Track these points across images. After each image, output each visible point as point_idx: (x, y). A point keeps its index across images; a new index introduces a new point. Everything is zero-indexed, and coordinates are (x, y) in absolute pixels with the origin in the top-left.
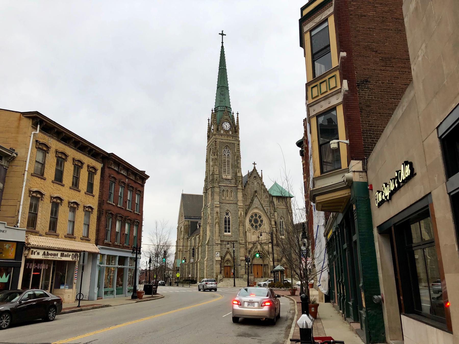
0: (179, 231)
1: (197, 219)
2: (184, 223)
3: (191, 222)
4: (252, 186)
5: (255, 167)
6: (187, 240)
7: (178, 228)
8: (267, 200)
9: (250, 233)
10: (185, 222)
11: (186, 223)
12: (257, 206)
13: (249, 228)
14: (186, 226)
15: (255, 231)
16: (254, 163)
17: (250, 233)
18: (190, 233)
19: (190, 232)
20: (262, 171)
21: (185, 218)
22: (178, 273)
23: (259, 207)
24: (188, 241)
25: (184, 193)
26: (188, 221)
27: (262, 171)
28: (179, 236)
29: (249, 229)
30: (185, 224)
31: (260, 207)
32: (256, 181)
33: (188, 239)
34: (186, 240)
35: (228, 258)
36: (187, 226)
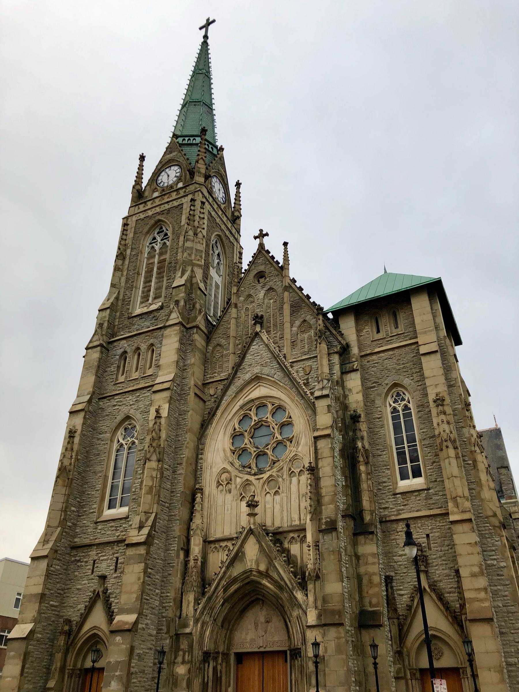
4: (247, 309)
5: (261, 246)
8: (310, 338)
9: (230, 491)
12: (257, 370)
13: (228, 472)
15: (252, 478)
16: (264, 232)
17: (230, 491)
20: (285, 244)
23: (266, 370)
27: (285, 244)
29: (225, 476)
31: (273, 372)
32: (263, 287)
35: (95, 628)
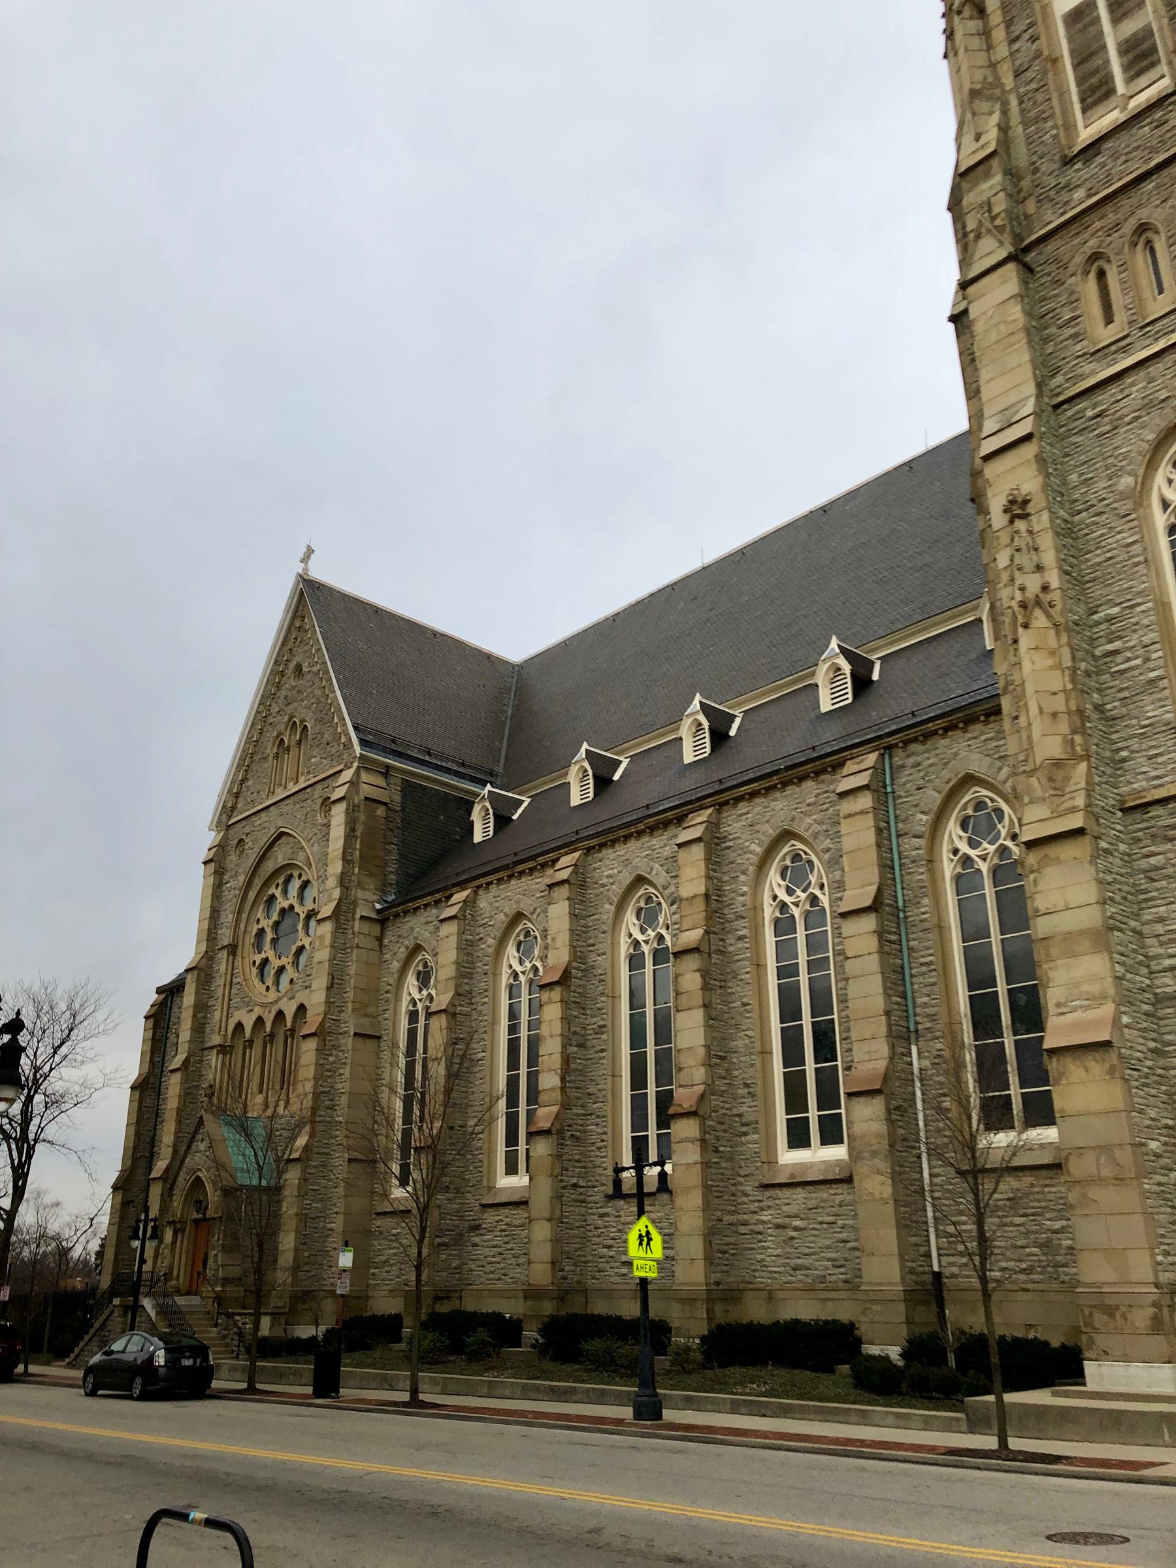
0: (234, 884)
1: (448, 771)
2: (354, 783)
3: (409, 788)
6: (376, 929)
7: (217, 862)
10: (365, 777)
11: (371, 785)
14: (371, 815)
18: (393, 878)
19: (392, 868)
21: (363, 743)
22: (643, 1224)
24: (380, 939)
25: (319, 572)
26: (387, 772)
28: (227, 917)
30: (365, 790)
33: (383, 920)
34: (366, 927)
36: (381, 811)
